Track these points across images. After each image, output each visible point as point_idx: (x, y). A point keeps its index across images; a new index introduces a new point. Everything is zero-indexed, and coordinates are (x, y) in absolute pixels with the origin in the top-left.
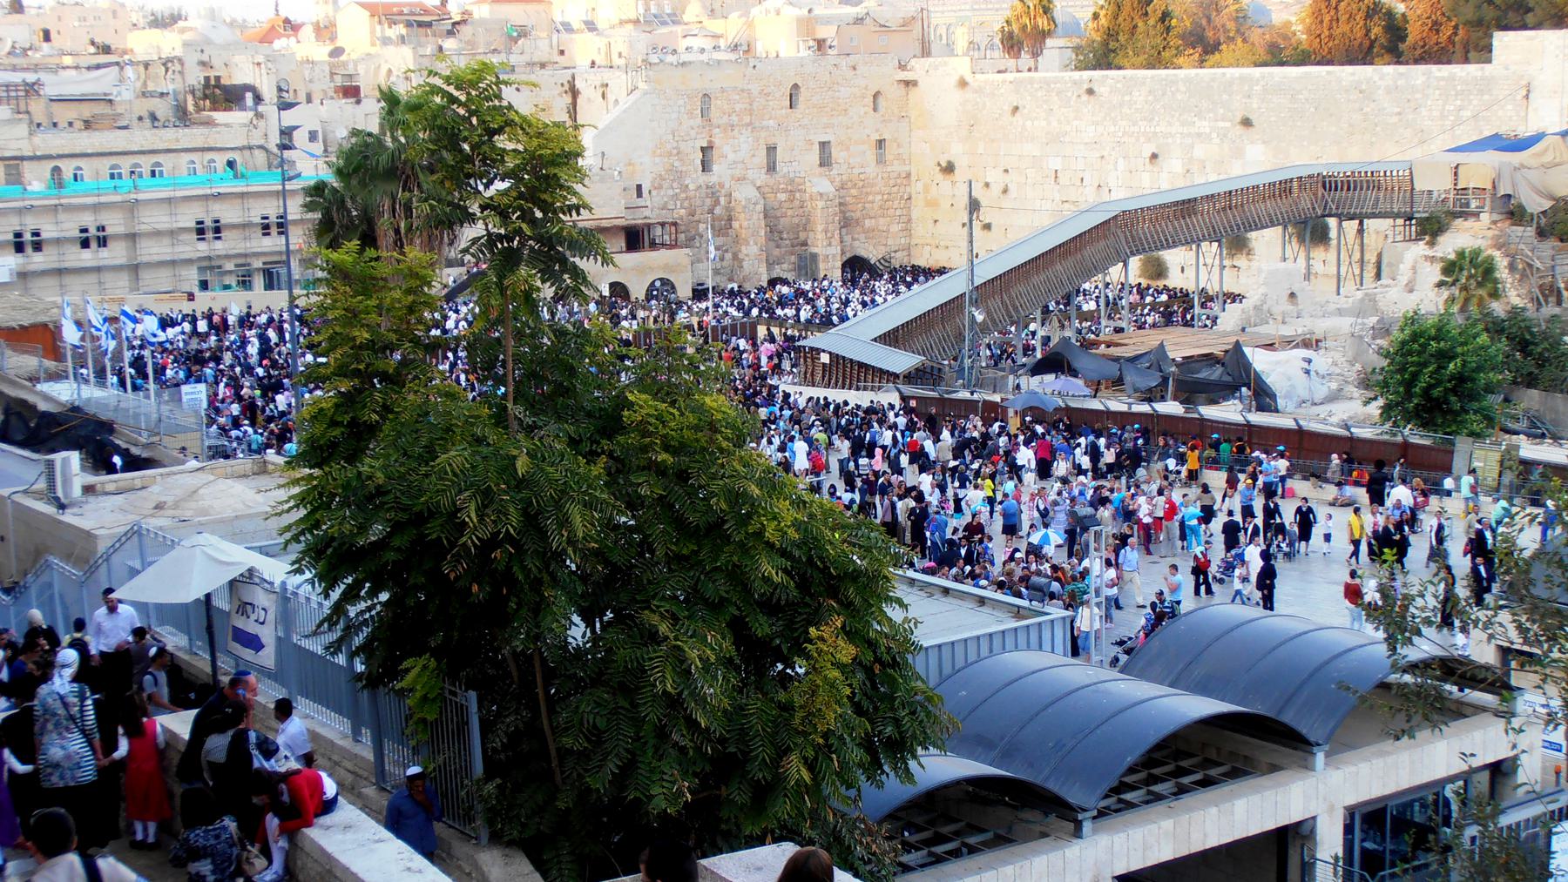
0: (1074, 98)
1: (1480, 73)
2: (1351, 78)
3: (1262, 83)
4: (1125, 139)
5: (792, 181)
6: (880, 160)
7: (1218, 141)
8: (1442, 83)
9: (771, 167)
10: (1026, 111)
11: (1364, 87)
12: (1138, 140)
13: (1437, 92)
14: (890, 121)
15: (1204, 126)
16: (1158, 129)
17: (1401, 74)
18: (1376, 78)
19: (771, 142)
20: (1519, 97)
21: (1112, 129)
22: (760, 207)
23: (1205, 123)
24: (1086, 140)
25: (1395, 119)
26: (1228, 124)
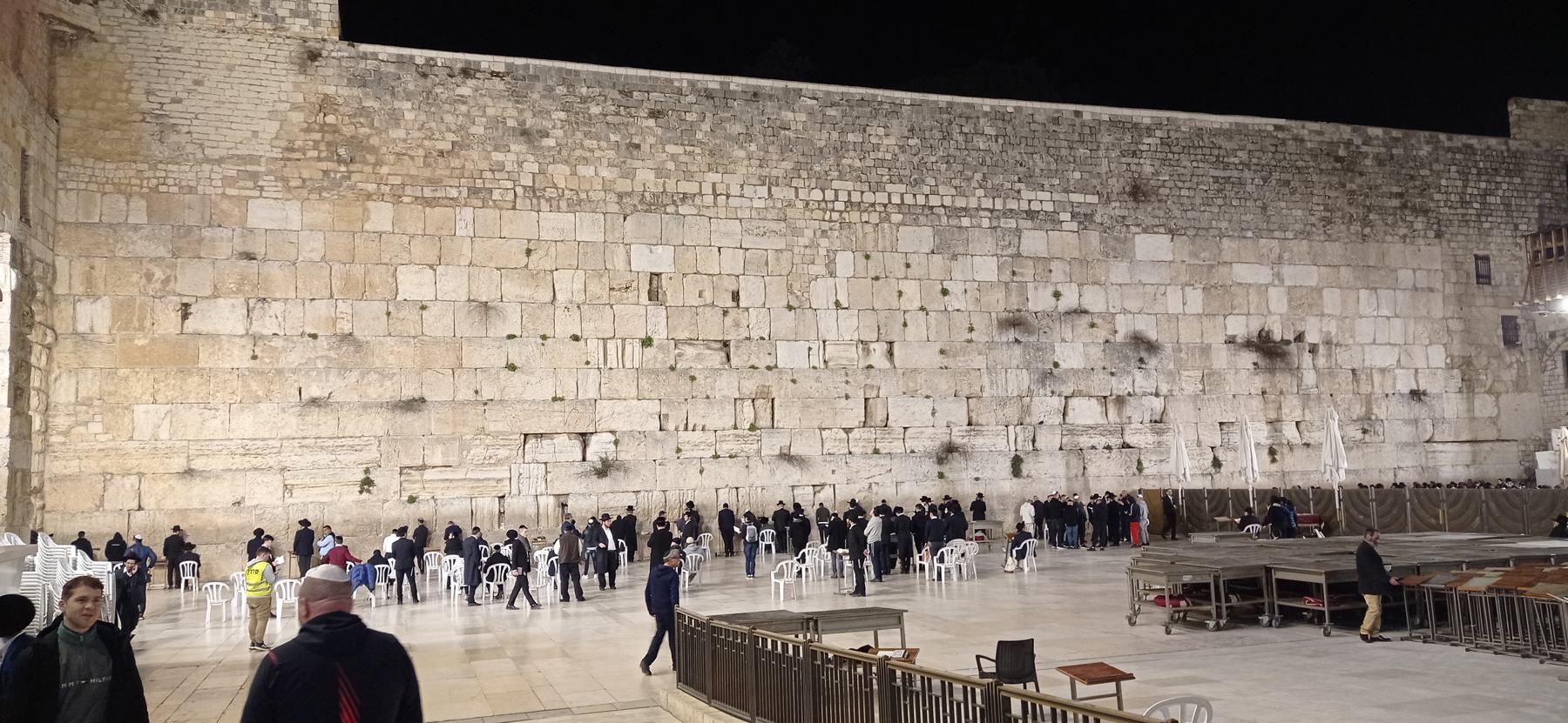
0: (706, 127)
2: (1319, 138)
4: (854, 216)
7: (1074, 226)
8: (1457, 156)
10: (550, 142)
11: (1342, 152)
12: (888, 219)
13: (1453, 168)
15: (1043, 200)
16: (934, 201)
17: (1396, 140)
18: (1358, 141)
21: (817, 195)
23: (1045, 196)
25: (1396, 203)
26: (1094, 199)
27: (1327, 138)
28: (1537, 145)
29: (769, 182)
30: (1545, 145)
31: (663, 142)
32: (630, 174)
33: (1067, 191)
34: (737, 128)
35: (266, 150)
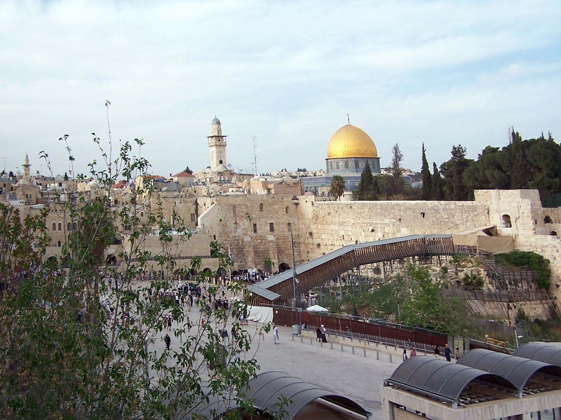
1: (472, 204)
3: (403, 206)
5: (262, 236)
6: (290, 230)
8: (460, 207)
9: (255, 231)
10: (332, 214)
11: (435, 208)
14: (292, 217)
15: (387, 221)
16: (373, 222)
17: (447, 204)
19: (254, 223)
20: (485, 213)
22: (252, 244)
23: (387, 220)
24: (351, 225)
26: (394, 220)
27: (433, 205)
28: (480, 203)
29: (354, 219)
30: (482, 203)
31: (342, 213)
32: (339, 219)
33: (391, 219)
34: (349, 210)
35: (311, 218)
